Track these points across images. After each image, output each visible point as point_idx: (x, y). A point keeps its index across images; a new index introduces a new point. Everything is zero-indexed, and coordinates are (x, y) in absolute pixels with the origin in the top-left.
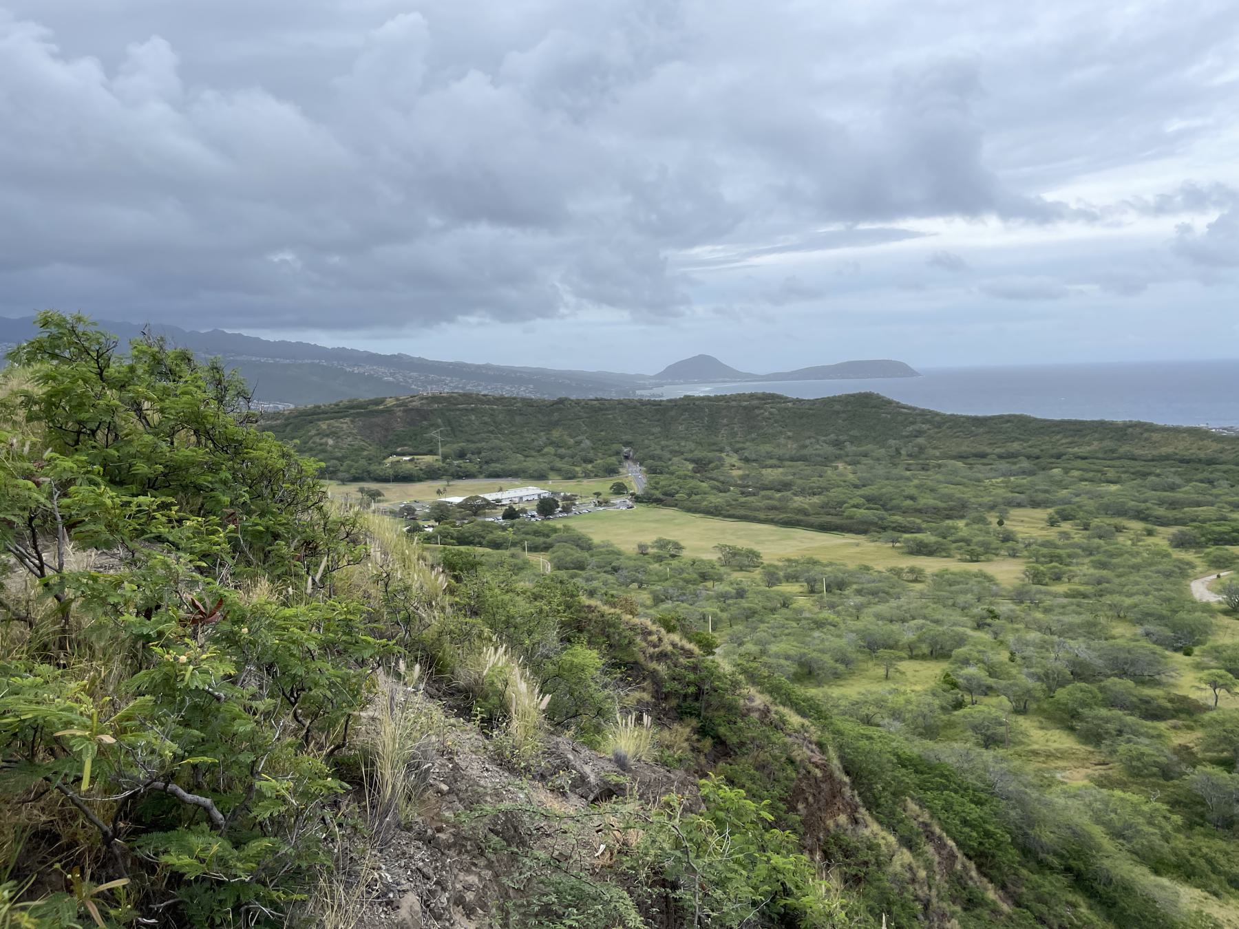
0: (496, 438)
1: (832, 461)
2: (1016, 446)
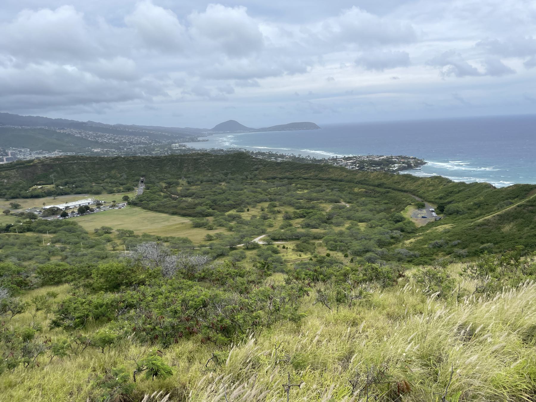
0: (85, 176)
1: (221, 182)
2: (287, 174)
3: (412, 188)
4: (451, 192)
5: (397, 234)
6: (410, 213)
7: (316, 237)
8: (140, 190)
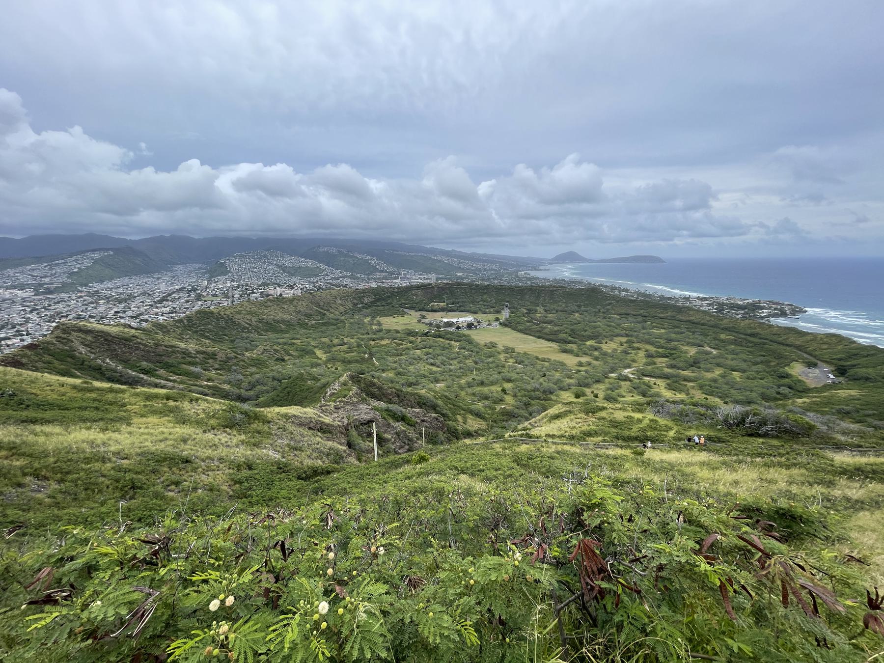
2: (642, 312)
3: (798, 343)
4: (856, 355)
5: (785, 390)
6: (797, 370)
7: (686, 379)
8: (505, 314)
